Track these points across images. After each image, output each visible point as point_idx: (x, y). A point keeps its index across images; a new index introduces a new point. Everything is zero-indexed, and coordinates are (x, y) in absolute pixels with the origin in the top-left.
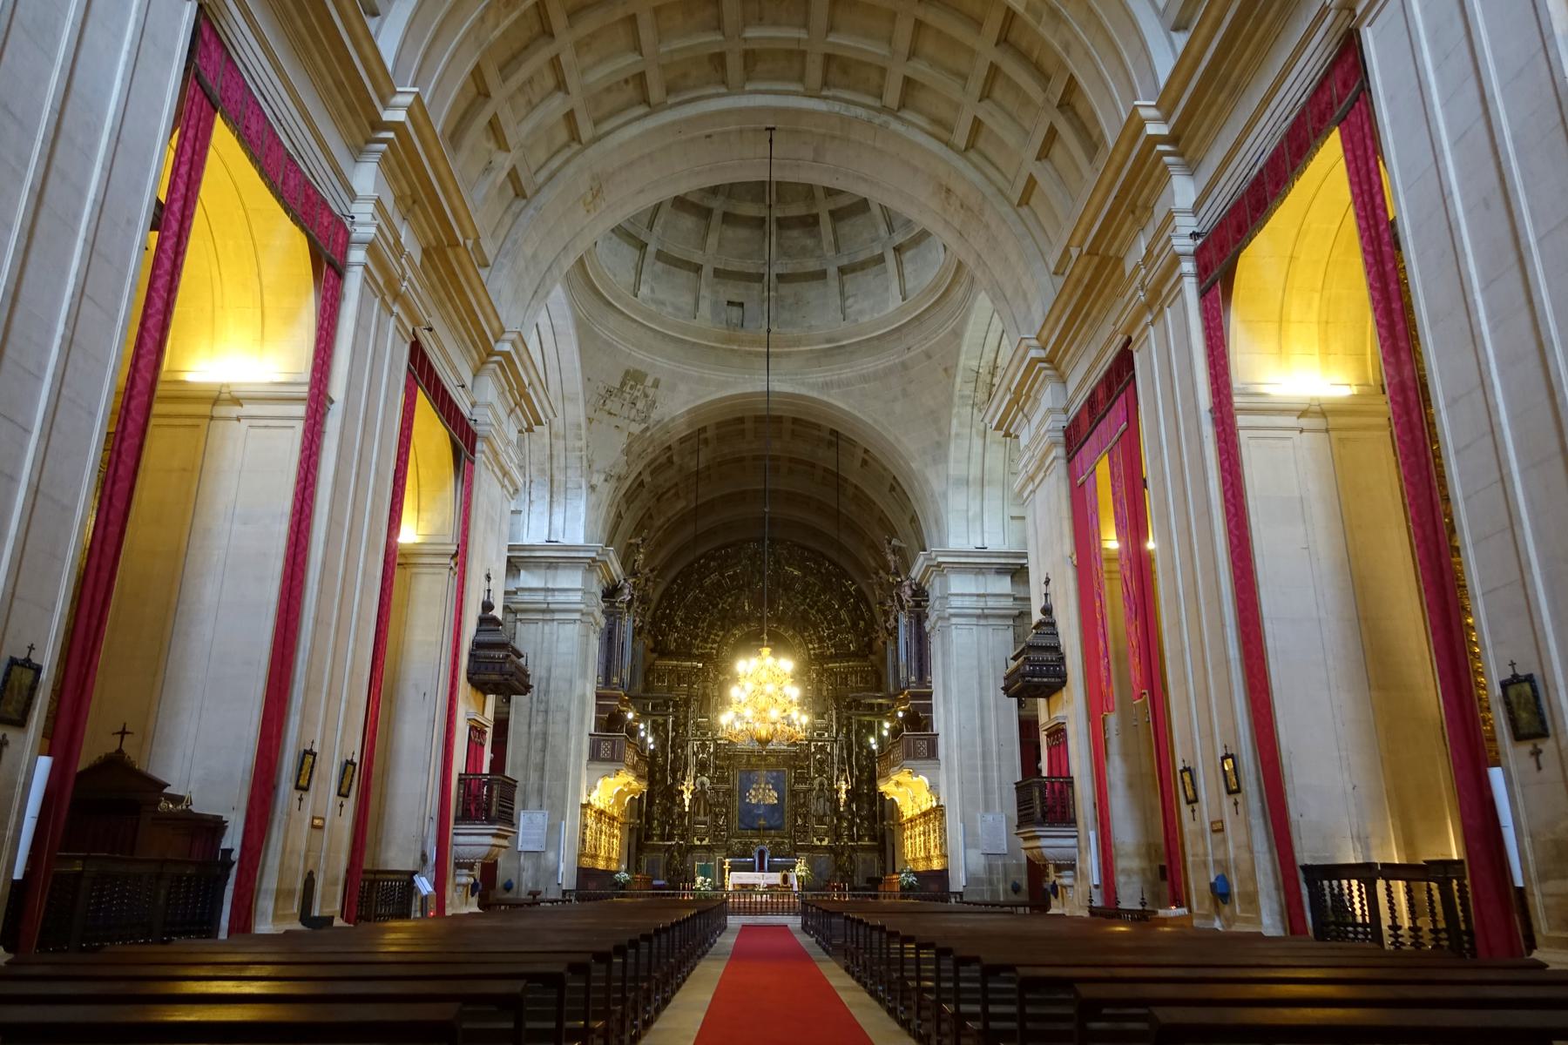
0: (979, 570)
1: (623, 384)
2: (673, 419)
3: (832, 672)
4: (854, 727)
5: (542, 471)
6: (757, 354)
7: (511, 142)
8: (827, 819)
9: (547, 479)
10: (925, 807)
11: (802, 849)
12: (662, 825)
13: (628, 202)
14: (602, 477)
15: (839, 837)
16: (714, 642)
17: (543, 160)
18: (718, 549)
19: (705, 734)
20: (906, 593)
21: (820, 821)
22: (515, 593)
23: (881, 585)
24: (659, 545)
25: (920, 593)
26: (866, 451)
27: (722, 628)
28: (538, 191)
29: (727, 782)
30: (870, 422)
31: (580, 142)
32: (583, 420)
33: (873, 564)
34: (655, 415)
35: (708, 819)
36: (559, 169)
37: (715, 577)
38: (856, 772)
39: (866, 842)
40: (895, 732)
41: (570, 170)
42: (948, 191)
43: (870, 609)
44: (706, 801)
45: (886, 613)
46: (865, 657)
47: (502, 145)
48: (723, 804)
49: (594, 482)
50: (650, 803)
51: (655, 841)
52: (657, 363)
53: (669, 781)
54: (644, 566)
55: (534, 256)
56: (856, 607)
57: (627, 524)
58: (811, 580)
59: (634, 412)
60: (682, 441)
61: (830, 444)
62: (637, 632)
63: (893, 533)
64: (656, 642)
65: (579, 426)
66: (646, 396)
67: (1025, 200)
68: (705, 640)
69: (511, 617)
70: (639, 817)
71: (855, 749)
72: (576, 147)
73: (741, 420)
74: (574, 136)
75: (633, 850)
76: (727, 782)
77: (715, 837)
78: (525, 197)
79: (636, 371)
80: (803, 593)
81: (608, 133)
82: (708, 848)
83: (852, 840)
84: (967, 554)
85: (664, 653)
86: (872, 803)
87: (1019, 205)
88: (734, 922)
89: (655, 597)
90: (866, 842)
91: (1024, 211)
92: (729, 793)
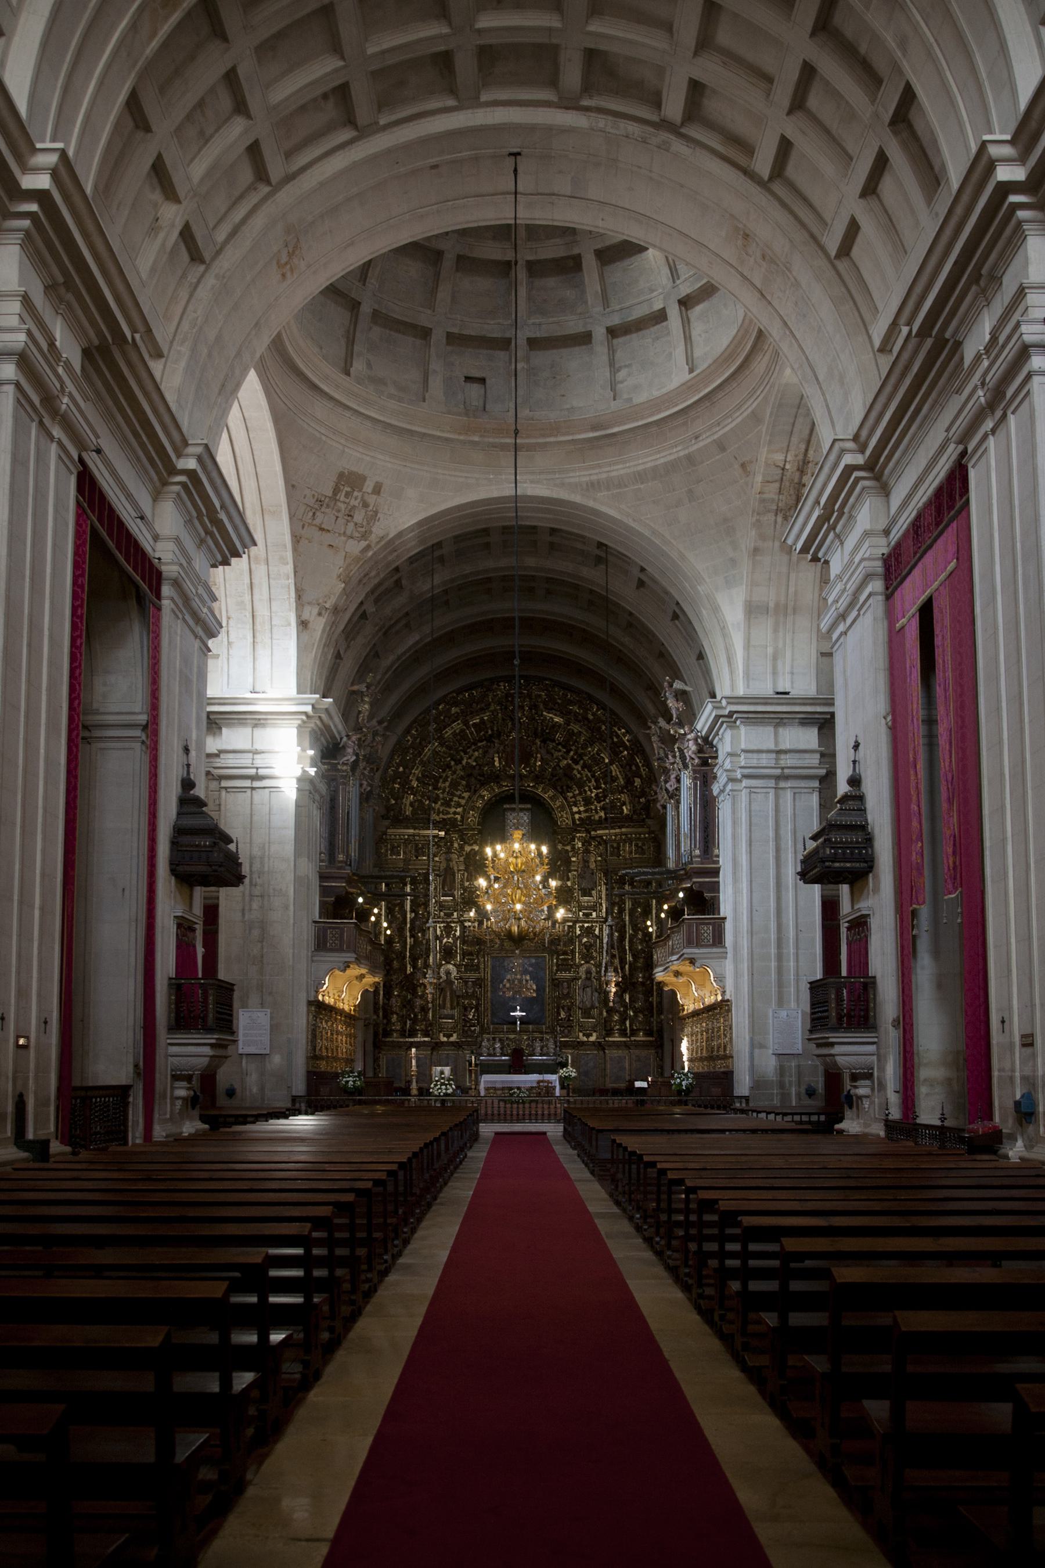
0: (779, 720)
1: (336, 491)
2: (400, 534)
3: (601, 841)
4: (628, 905)
5: (241, 604)
6: (503, 447)
7: (181, 190)
8: (595, 1012)
9: (249, 615)
10: (710, 1000)
11: (565, 1045)
12: (402, 1019)
13: (334, 259)
14: (315, 611)
15: (609, 1033)
16: (459, 805)
17: (223, 210)
18: (460, 691)
19: (450, 915)
20: (691, 748)
21: (587, 1013)
22: (217, 755)
23: (662, 740)
24: (388, 688)
25: (707, 748)
26: (643, 570)
27: (468, 788)
28: (218, 252)
29: (477, 969)
30: (647, 533)
31: (268, 182)
32: (288, 539)
33: (652, 710)
34: (378, 530)
35: (456, 1012)
36: (244, 221)
37: (457, 726)
38: (629, 958)
39: (641, 1037)
40: (675, 914)
41: (259, 221)
42: (746, 236)
43: (648, 764)
44: (453, 992)
45: (666, 771)
46: (641, 823)
47: (170, 194)
48: (473, 995)
49: (306, 616)
50: (388, 994)
51: (395, 1037)
52: (377, 463)
53: (409, 970)
54: (371, 717)
55: (219, 338)
56: (631, 762)
57: (348, 666)
58: (575, 728)
59: (351, 526)
60: (412, 560)
61: (599, 560)
62: (365, 798)
63: (677, 675)
64: (389, 808)
65: (285, 546)
66: (366, 505)
67: (845, 249)
68: (447, 804)
69: (214, 785)
70: (376, 1012)
71: (629, 931)
72: (265, 189)
73: (486, 531)
74: (261, 175)
75: (370, 1047)
76: (478, 965)
77: (464, 1033)
78: (202, 261)
79: (351, 473)
80: (566, 745)
81: (303, 169)
82: (457, 1045)
83: (624, 1035)
84: (765, 701)
85: (399, 820)
86: (649, 992)
87: (838, 256)
88: (487, 1130)
89: (384, 753)
90: (641, 1037)
91: (842, 265)
92: (479, 983)
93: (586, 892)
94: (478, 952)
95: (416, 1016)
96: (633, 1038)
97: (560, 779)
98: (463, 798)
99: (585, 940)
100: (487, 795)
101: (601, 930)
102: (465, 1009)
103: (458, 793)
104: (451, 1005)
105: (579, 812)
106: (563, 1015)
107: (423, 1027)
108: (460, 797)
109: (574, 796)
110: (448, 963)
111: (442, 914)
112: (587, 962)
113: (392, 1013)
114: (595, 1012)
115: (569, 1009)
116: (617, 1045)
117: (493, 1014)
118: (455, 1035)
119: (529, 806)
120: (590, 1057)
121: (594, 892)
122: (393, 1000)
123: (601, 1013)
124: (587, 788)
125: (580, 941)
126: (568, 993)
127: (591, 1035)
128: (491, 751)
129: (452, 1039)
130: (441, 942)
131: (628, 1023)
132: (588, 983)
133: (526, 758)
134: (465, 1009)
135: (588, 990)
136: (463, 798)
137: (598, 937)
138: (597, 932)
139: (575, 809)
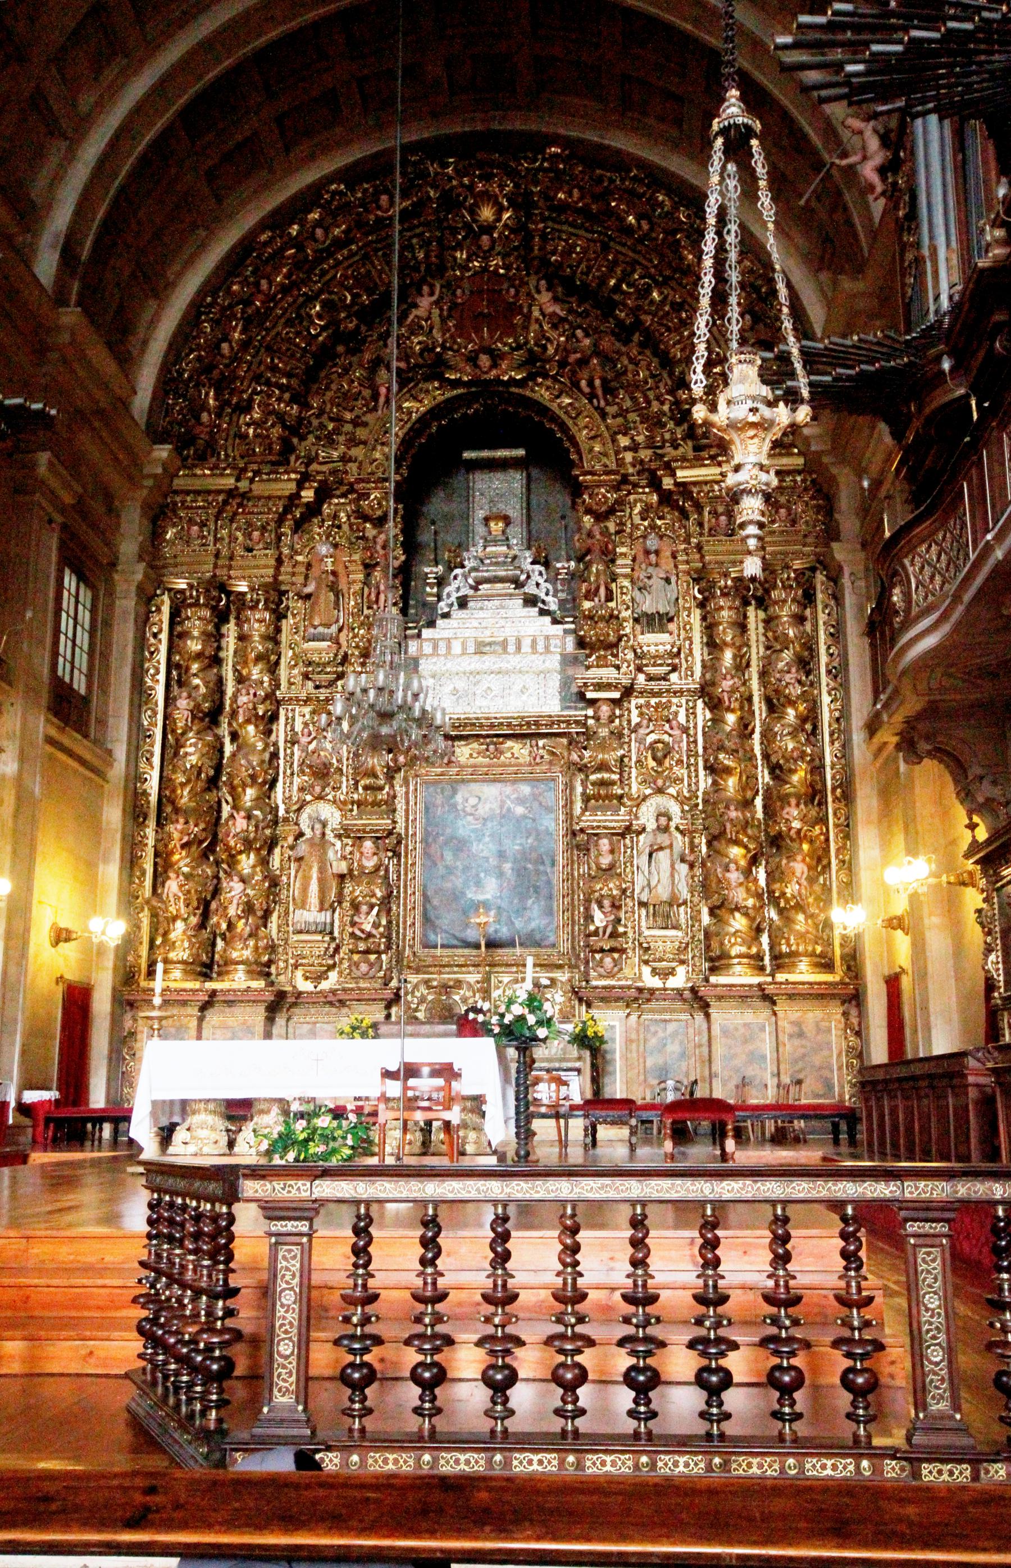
11: (609, 997)
15: (718, 962)
16: (353, 442)
21: (663, 913)
38: (764, 777)
90: (804, 973)
93: (656, 621)
94: (391, 773)
95: (231, 926)
96: (780, 977)
97: (584, 362)
98: (365, 424)
99: (652, 737)
100: (416, 407)
101: (691, 712)
102: (356, 907)
103: (348, 416)
104: (322, 902)
105: (634, 448)
106: (600, 919)
107: (247, 954)
108: (356, 423)
109: (623, 413)
110: (320, 798)
111: (310, 684)
112: (660, 791)
113: (174, 919)
114: (683, 915)
115: (616, 907)
116: (742, 996)
117: (426, 919)
118: (333, 975)
119: (521, 452)
120: (671, 1027)
121: (672, 626)
122: (172, 886)
123: (696, 918)
124: (651, 395)
125: (641, 741)
126: (612, 867)
127: (672, 972)
128: (425, 302)
129: (325, 985)
130: (304, 750)
131: (765, 939)
132: (663, 839)
133: (506, 315)
134: (356, 907)
135: (663, 857)
136: (365, 424)
137: (685, 730)
138: (682, 719)
139: (624, 441)
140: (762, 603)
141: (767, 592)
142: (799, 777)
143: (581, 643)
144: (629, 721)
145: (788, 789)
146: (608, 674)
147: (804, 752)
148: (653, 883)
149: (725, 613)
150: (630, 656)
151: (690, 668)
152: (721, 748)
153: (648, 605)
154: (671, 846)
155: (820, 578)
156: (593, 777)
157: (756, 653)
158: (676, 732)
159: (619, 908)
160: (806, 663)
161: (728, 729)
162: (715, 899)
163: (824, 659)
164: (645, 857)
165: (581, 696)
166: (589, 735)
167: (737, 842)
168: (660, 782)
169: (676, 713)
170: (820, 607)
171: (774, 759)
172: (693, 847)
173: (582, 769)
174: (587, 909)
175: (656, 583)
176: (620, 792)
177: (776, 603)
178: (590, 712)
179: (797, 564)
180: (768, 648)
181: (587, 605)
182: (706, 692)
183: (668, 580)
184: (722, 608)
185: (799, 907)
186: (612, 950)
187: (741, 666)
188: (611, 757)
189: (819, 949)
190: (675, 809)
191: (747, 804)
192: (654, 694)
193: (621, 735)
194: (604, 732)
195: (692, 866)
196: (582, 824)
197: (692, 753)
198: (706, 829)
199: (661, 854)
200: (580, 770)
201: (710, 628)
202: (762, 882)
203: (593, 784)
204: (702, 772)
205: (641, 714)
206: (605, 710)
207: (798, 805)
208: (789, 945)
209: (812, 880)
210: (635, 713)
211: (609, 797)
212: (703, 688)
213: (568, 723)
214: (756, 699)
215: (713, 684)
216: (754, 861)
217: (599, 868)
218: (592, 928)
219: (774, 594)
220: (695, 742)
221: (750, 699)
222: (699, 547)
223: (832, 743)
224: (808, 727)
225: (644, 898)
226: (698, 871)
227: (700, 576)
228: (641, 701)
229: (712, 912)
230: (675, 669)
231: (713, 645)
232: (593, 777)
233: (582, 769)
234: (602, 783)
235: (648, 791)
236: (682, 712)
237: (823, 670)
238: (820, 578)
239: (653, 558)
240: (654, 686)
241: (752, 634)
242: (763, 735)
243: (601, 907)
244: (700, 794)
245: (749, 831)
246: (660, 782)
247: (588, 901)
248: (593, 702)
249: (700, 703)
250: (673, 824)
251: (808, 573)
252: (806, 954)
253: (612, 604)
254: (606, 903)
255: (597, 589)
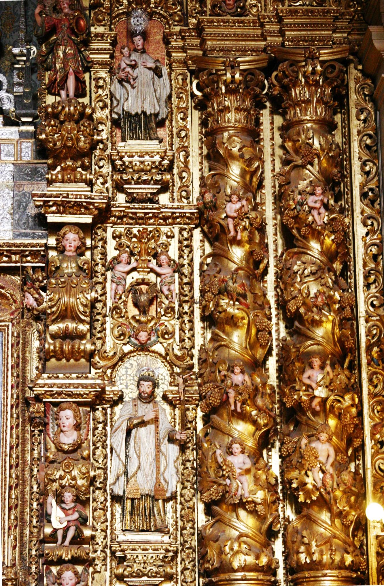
38: (279, 331)
101: (186, 245)
106: (58, 518)
112: (143, 348)
114: (170, 514)
115: (81, 501)
121: (162, 133)
123: (188, 517)
126: (77, 447)
131: (278, 546)
132: (146, 411)
135: (145, 436)
138: (173, 252)
140: (279, 107)
141: (286, 89)
142: (324, 330)
143: (42, 151)
144: (104, 254)
145: (310, 346)
146: (77, 190)
147: (331, 297)
148: (131, 470)
149: (232, 117)
150: (107, 169)
151: (185, 188)
152: (224, 291)
153: (132, 102)
154: (156, 420)
155: (354, 73)
156: (53, 328)
157: (271, 168)
158: (166, 270)
159: (85, 503)
160: (334, 182)
161: (233, 267)
162: (214, 492)
163: (358, 178)
164: (121, 435)
165: (40, 220)
166: (50, 271)
167: (243, 416)
168: (143, 336)
169: (166, 246)
170: (353, 111)
171: (292, 306)
172: (185, 423)
173: (39, 317)
174: (42, 505)
175: (142, 74)
176: (89, 347)
177: (297, 104)
178: (52, 241)
179: (325, 55)
180: (285, 162)
181: (50, 100)
182: (206, 219)
183: (157, 72)
184: (227, 109)
185: (324, 503)
186: (75, 561)
187: (252, 186)
188: (79, 301)
189: (349, 559)
190: (162, 372)
191: (257, 366)
192: (137, 220)
193: (92, 273)
194: (69, 268)
195: (183, 448)
196: (38, 390)
197: (186, 298)
198: (202, 398)
199: (142, 431)
200: (37, 319)
201: (211, 134)
202: (276, 470)
203: (54, 337)
204: (198, 324)
205: (119, 247)
206: (72, 239)
207: (322, 367)
208: (310, 554)
209: (340, 467)
210: (111, 244)
211: (75, 355)
212: (201, 213)
213: (22, 254)
214: (270, 230)
215: (215, 207)
216: (264, 442)
217: (60, 449)
218: (48, 530)
219: (296, 93)
220: (190, 284)
221: (262, 229)
222: (199, 29)
223: (368, 286)
224: (337, 266)
225: (119, 490)
226: (191, 455)
227: (201, 68)
228: (121, 229)
229: (209, 512)
230: (165, 188)
231: (215, 157)
232: (53, 328)
233: (39, 317)
234: (67, 336)
235: (127, 348)
236: (174, 244)
237: (357, 193)
238: (354, 73)
239: (138, 41)
240: (139, 209)
241: (266, 145)
242: (278, 276)
243: (60, 501)
244: (196, 352)
245: (259, 402)
246: (143, 336)
247: (43, 493)
248: (55, 229)
249: (197, 234)
250: (159, 392)
251: (338, 66)
252: (332, 566)
253: (85, 100)
254: (68, 496)
255: (65, 79)
